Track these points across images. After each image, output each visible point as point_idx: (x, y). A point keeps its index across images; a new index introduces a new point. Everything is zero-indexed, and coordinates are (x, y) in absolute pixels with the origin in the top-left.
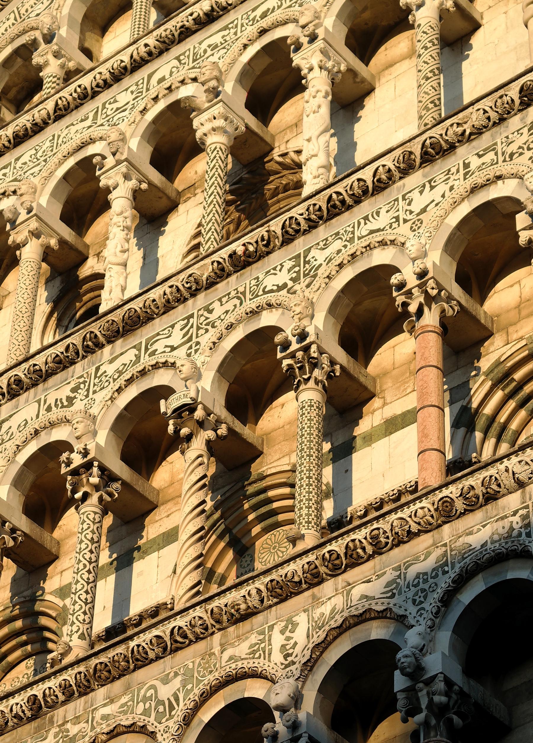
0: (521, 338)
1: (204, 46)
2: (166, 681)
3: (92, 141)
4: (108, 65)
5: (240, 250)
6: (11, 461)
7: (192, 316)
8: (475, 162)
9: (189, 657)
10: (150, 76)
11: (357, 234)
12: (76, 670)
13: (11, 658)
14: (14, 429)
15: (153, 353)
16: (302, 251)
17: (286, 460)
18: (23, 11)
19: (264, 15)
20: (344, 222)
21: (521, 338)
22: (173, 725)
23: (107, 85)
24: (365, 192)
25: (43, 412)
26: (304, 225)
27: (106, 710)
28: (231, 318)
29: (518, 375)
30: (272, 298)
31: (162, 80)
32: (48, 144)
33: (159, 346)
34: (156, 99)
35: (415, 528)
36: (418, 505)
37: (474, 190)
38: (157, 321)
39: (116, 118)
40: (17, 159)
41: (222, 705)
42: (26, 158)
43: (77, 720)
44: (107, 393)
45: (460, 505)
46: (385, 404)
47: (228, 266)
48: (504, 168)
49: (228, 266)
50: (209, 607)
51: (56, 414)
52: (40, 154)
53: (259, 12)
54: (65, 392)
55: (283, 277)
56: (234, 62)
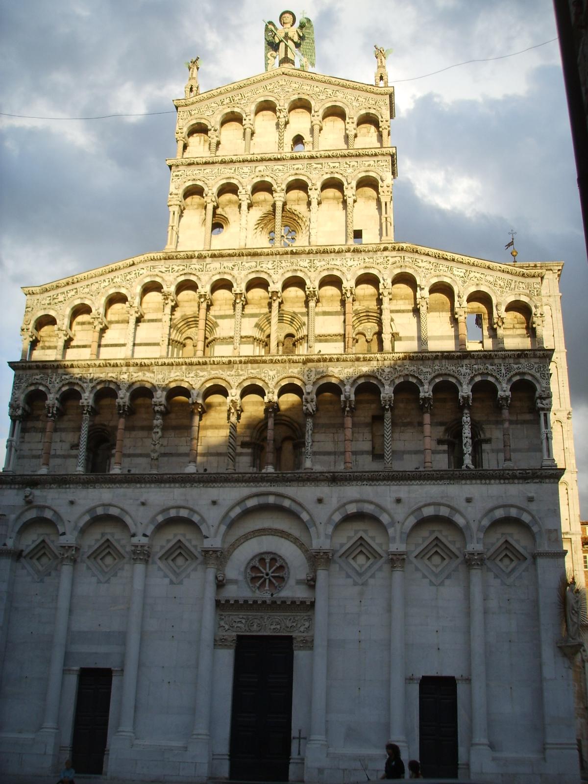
0: (364, 306)
1: (276, 167)
2: (271, 370)
3: (233, 178)
4: (243, 157)
5: (294, 251)
6: (211, 279)
7: (274, 261)
8: (367, 260)
9: (278, 366)
10: (256, 167)
11: (330, 263)
12: (245, 358)
13: (191, 326)
14: (212, 268)
15: (262, 267)
16: (312, 259)
17: (291, 309)
18: (201, 110)
19: (297, 169)
20: (327, 257)
21: (364, 306)
22: (274, 383)
23: (240, 162)
24: (334, 252)
25: (222, 267)
26: (314, 252)
27: (253, 371)
28: (289, 269)
29: (361, 315)
30: (302, 269)
31: (260, 171)
32: (216, 170)
33: (264, 266)
34: (257, 176)
35: (349, 360)
36: (352, 356)
37: (366, 267)
38: (263, 257)
39: (243, 176)
40: (204, 170)
41: (287, 383)
42: (208, 171)
43: (242, 370)
44: (246, 272)
45: (362, 359)
46: (323, 306)
47: (289, 252)
48: (374, 265)
49: (289, 252)
50: (289, 357)
51: (227, 270)
52: (213, 172)
53: (296, 167)
54: (230, 265)
55: (306, 264)
56: (286, 179)
